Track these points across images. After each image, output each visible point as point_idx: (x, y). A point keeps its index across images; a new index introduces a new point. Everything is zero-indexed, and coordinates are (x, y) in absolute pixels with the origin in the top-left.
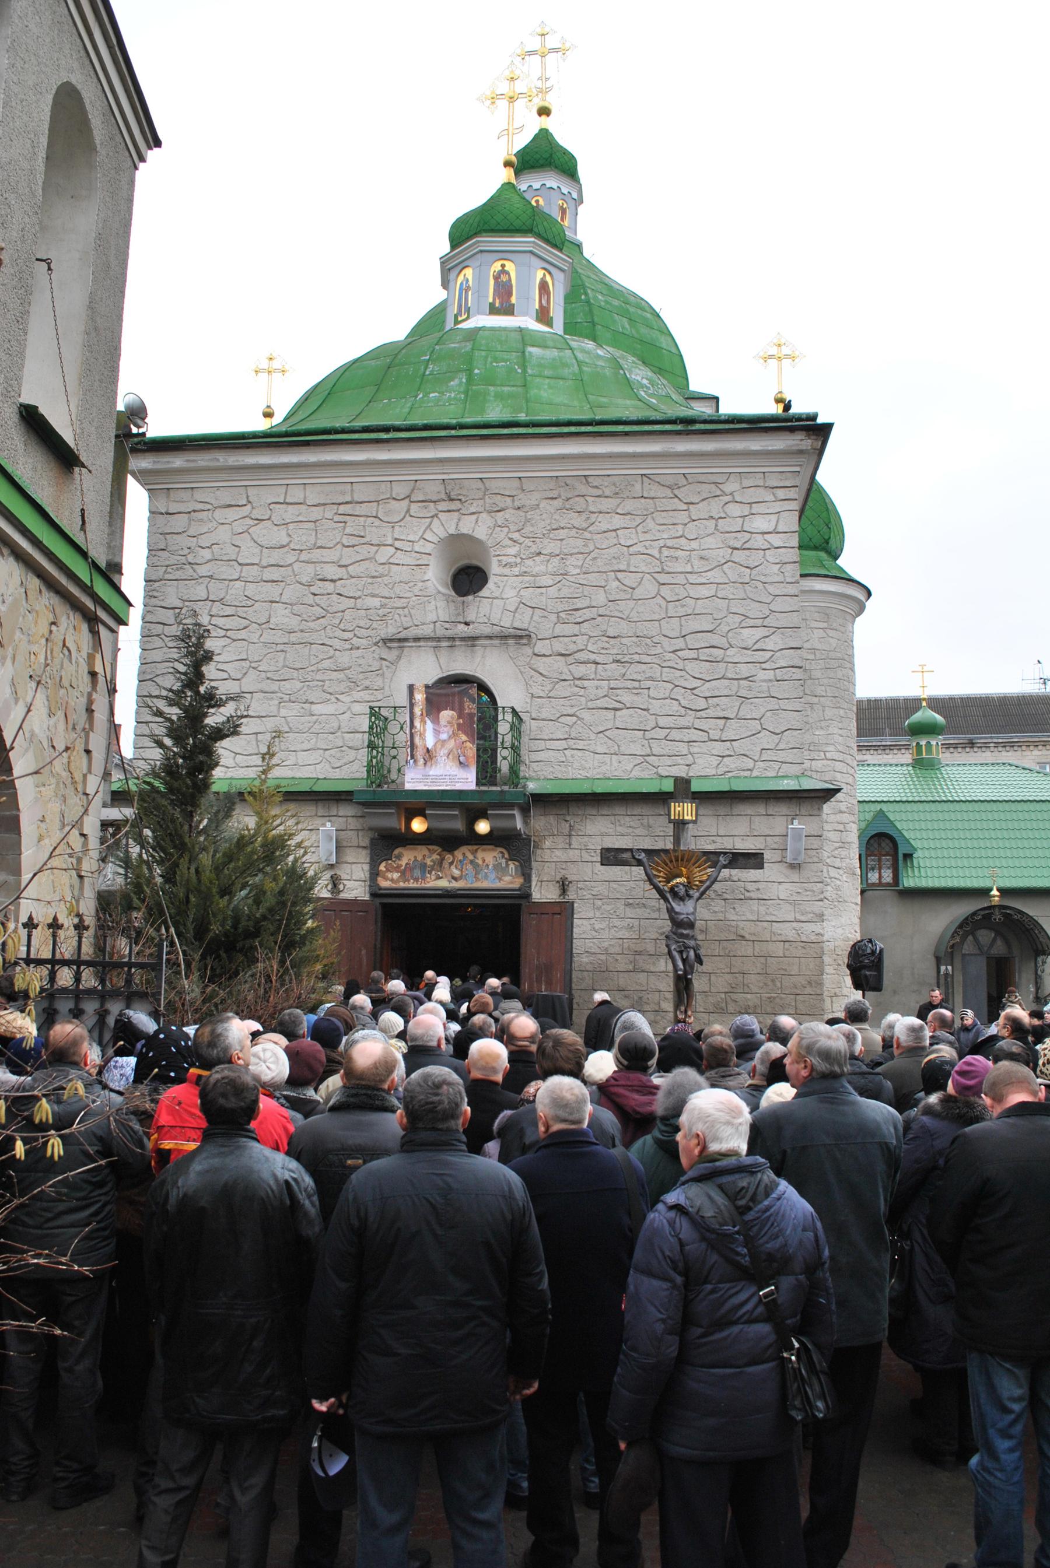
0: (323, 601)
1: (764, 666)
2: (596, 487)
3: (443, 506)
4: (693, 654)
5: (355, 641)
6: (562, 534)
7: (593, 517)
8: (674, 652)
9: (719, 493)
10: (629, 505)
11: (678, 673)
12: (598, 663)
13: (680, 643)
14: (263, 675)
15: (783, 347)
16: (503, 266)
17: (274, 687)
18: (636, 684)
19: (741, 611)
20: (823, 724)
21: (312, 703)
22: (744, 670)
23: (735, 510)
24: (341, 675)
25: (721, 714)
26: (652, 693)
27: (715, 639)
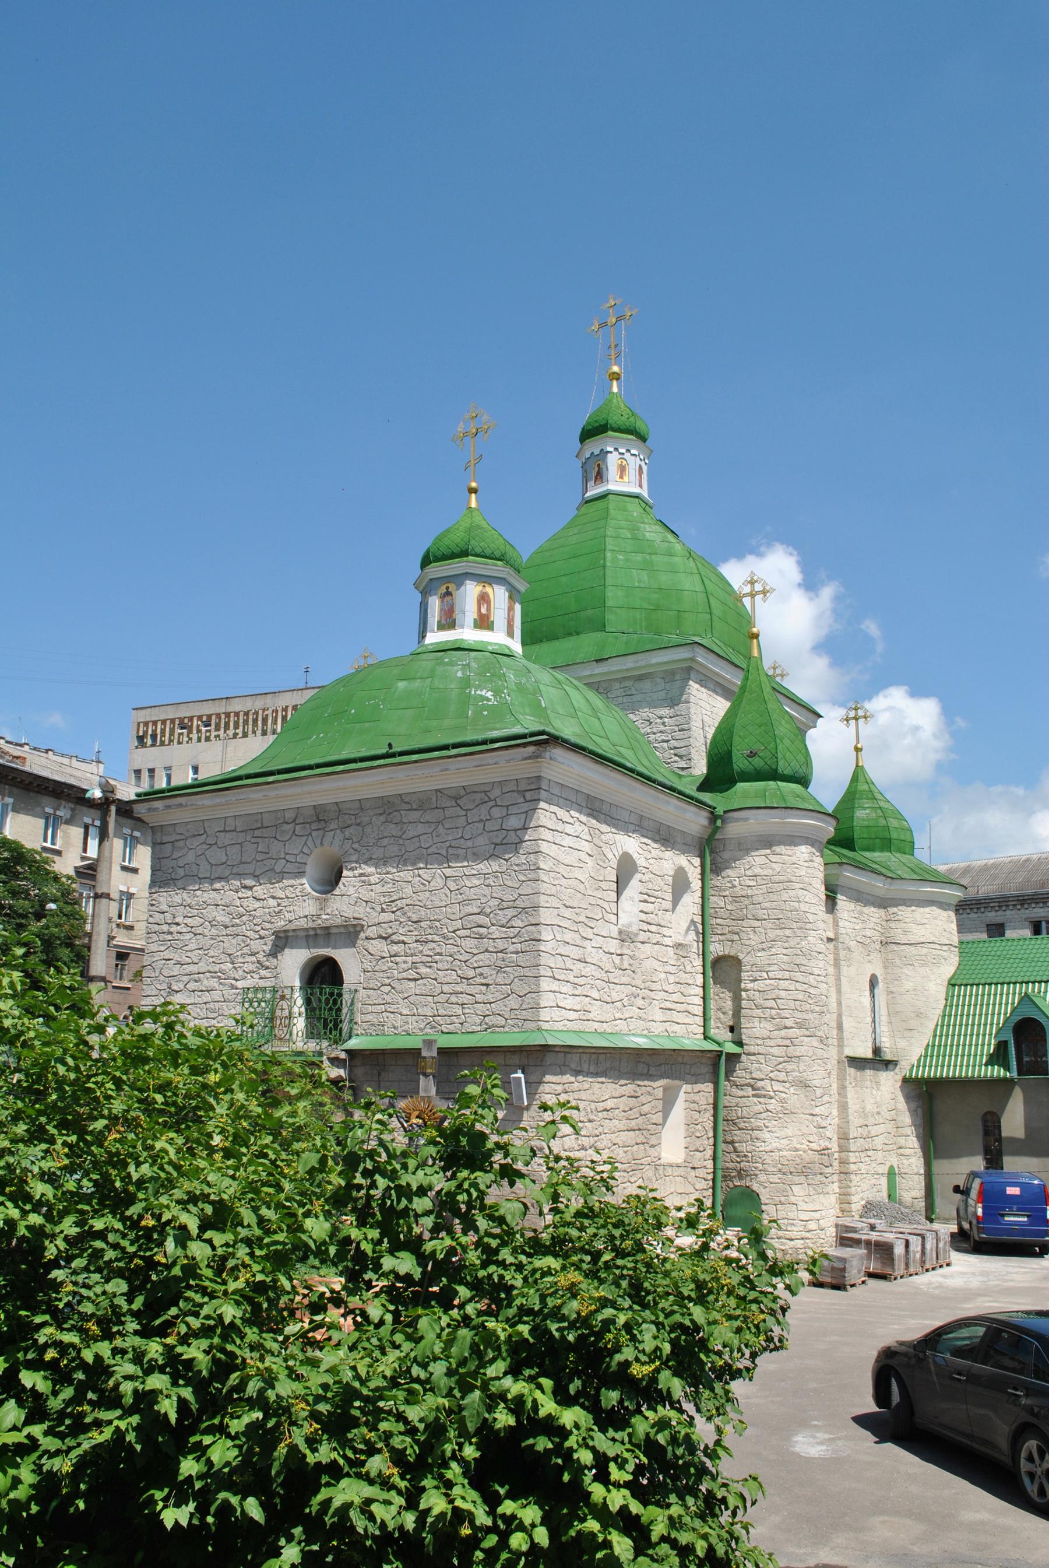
0: (245, 903)
1: (514, 940)
2: (408, 803)
3: (314, 826)
4: (467, 933)
5: (262, 933)
6: (385, 842)
7: (405, 826)
8: (454, 932)
9: (486, 799)
10: (428, 816)
11: (456, 949)
12: (404, 943)
13: (458, 924)
14: (211, 960)
15: (756, 585)
16: (447, 588)
17: (217, 968)
18: (429, 959)
19: (499, 895)
20: (764, 946)
21: (237, 980)
22: (501, 945)
23: (496, 812)
24: (254, 959)
25: (484, 981)
26: (440, 966)
27: (483, 920)
